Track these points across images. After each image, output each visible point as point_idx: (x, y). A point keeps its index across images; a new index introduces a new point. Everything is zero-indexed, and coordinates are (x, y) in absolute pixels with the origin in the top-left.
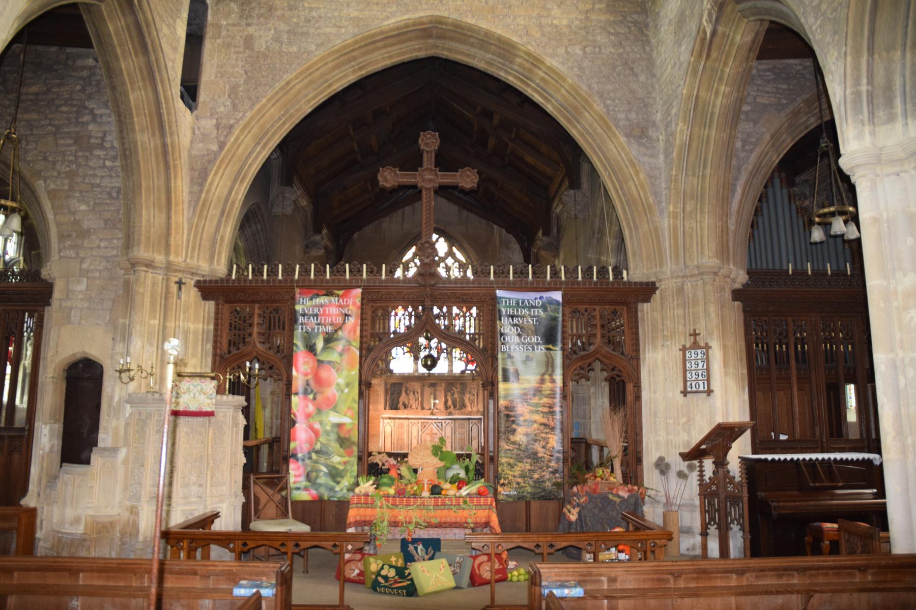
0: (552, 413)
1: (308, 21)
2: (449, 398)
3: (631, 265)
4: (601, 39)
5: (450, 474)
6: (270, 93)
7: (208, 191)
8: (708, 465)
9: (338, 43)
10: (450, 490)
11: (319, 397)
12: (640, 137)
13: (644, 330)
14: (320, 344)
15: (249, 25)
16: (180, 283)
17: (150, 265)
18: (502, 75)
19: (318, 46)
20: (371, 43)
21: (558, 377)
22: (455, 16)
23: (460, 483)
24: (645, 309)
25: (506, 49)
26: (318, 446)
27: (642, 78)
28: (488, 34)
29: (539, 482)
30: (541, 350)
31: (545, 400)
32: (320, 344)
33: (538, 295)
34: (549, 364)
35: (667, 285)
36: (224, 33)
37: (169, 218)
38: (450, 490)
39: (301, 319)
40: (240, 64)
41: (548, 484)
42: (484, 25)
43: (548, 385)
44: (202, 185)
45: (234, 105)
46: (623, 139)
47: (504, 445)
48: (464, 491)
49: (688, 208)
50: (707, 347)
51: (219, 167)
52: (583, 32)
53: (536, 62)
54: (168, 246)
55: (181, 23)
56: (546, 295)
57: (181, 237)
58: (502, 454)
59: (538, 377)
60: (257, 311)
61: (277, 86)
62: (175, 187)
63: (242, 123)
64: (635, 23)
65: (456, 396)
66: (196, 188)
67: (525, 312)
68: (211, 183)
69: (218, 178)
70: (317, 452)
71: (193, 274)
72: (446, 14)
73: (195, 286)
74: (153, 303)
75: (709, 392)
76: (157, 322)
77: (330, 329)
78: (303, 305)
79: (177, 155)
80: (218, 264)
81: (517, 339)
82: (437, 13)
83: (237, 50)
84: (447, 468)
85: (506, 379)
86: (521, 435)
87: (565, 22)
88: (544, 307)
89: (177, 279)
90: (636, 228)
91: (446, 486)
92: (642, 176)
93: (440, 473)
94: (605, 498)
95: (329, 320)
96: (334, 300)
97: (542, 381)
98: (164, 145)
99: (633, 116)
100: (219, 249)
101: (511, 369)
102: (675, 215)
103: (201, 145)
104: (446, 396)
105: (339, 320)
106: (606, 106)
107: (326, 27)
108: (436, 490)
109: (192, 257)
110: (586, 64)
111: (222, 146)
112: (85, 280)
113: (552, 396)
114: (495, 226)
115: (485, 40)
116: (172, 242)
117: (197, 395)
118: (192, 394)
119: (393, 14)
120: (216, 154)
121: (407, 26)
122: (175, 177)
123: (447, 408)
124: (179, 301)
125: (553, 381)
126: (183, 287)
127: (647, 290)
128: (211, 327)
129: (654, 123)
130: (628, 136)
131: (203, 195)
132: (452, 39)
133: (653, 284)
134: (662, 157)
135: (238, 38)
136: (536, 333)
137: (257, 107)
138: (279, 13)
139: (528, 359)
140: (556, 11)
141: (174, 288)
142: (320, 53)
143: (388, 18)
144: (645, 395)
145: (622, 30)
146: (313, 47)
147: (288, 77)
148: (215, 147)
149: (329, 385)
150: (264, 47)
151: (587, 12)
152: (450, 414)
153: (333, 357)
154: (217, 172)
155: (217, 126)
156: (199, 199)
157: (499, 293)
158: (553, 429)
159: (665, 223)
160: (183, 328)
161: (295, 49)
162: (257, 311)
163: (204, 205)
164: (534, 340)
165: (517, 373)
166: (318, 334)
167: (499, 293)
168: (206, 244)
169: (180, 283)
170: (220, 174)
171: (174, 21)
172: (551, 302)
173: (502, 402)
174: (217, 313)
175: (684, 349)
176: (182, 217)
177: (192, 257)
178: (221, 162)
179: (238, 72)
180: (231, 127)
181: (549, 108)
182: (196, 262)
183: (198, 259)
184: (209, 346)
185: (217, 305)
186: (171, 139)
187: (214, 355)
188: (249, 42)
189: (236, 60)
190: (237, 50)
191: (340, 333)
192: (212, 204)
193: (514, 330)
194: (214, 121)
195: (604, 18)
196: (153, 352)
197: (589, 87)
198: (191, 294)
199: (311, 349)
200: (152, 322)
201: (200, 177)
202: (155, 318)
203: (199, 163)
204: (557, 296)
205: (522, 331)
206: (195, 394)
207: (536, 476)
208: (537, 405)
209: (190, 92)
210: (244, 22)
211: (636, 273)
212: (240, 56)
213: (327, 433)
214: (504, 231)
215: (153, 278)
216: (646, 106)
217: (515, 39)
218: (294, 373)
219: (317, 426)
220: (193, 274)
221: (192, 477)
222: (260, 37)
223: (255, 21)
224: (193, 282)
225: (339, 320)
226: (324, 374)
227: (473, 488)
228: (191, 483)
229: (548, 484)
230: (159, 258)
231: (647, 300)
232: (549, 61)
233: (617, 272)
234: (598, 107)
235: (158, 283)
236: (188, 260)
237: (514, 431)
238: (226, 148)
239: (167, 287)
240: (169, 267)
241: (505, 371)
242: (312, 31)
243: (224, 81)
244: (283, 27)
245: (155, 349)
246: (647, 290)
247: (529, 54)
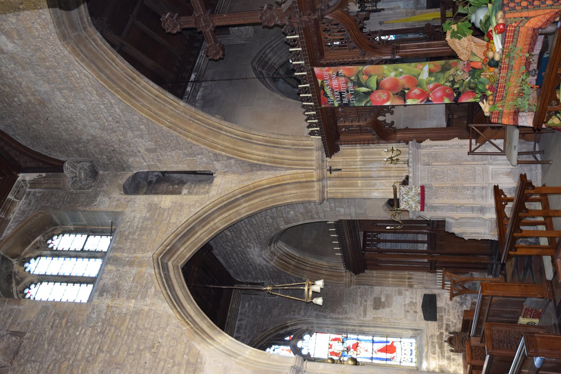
7: (264, 161)
15: (139, 152)
16: (330, 170)
40: (169, 153)
51: (245, 158)
55: (163, 203)
62: (267, 184)
68: (258, 160)
69: (253, 156)
71: (323, 161)
73: (331, 158)
76: (359, 182)
79: (246, 188)
80: (313, 146)
83: (160, 156)
89: (329, 173)
100: (302, 146)
103: (234, 168)
107: (116, 111)
109: (311, 165)
112: (337, 209)
117: (409, 197)
118: (409, 200)
120: (236, 160)
122: (262, 185)
124: (343, 170)
126: (333, 168)
131: (267, 164)
135: (151, 156)
137: (194, 142)
141: (335, 174)
148: (233, 161)
150: (150, 143)
154: (249, 158)
156: (271, 166)
160: (361, 165)
163: (274, 163)
170: (250, 155)
171: (164, 210)
176: (285, 175)
177: (311, 165)
178: (241, 157)
179: (175, 154)
180: (215, 155)
182: (314, 162)
183: (312, 160)
185: (341, 144)
186: (238, 195)
189: (168, 156)
190: (160, 156)
192: (271, 155)
194: (214, 162)
196: (380, 183)
198: (337, 160)
200: (360, 185)
202: (357, 183)
203: (246, 168)
206: (409, 198)
212: (163, 154)
215: (330, 187)
220: (323, 161)
221: (468, 193)
222: (145, 145)
223: (135, 149)
224: (328, 159)
228: (472, 194)
235: (334, 183)
236: (314, 168)
238: (231, 156)
239: (335, 178)
243: (185, 160)
244: (130, 134)
245: (378, 181)
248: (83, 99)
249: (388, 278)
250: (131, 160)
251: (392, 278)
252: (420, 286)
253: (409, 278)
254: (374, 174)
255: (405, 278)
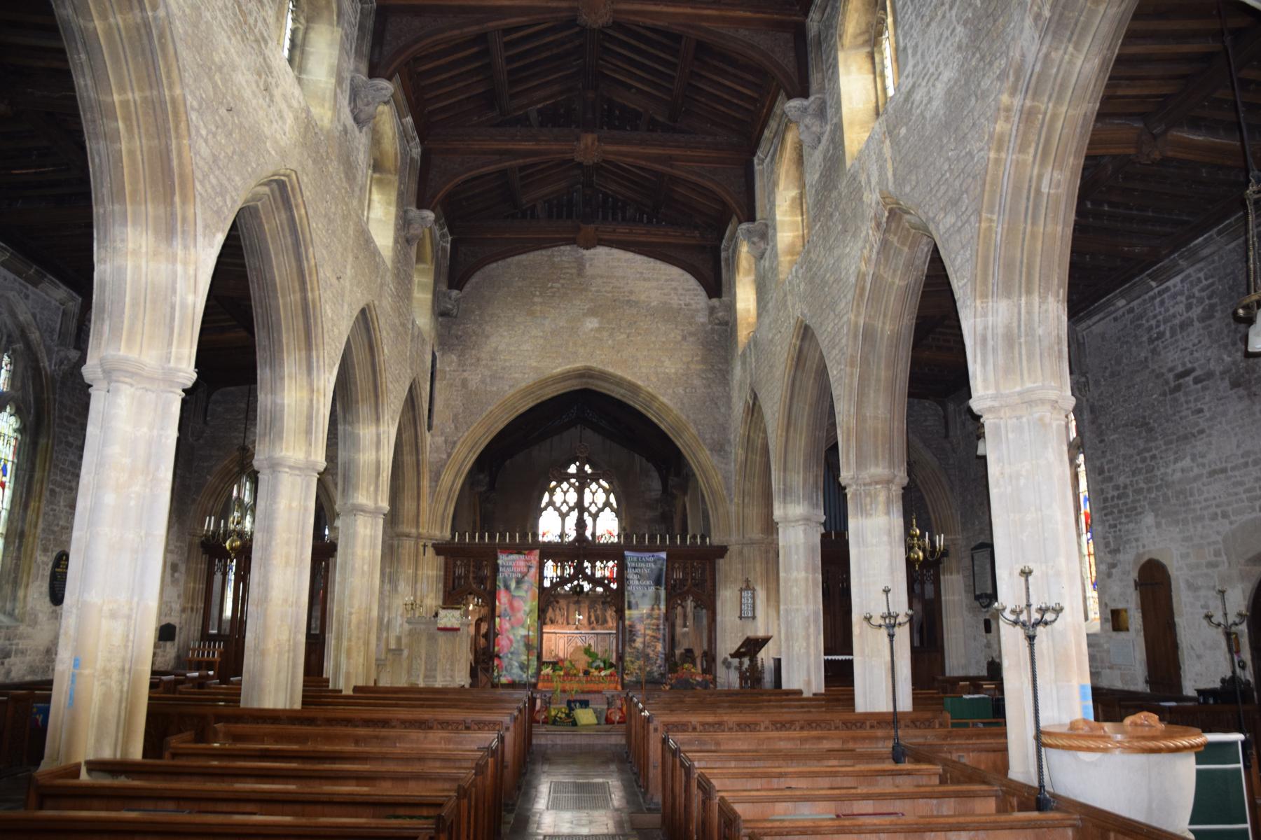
0: (658, 629)
1: (504, 368)
2: (592, 614)
3: (713, 534)
4: (697, 382)
5: (595, 665)
6: (480, 419)
8: (746, 661)
9: (523, 385)
10: (595, 672)
11: (513, 619)
12: (720, 451)
13: (719, 577)
14: (513, 585)
15: (464, 371)
16: (425, 546)
17: (408, 536)
18: (631, 403)
19: (510, 387)
20: (544, 383)
21: (663, 607)
22: (600, 367)
23: (599, 669)
24: (721, 562)
25: (634, 388)
26: (512, 649)
27: (723, 410)
28: (621, 379)
29: (650, 673)
30: (652, 589)
31: (654, 621)
32: (513, 585)
33: (651, 554)
34: (657, 598)
35: (733, 549)
36: (448, 376)
37: (418, 505)
38: (595, 672)
39: (501, 569)
40: (460, 399)
41: (656, 674)
42: (619, 373)
43: (656, 612)
44: (437, 481)
45: (456, 428)
46: (708, 452)
47: (628, 649)
48: (603, 673)
49: (746, 501)
50: (754, 590)
52: (685, 378)
53: (653, 398)
54: (418, 522)
56: (656, 554)
57: (425, 517)
58: (627, 655)
59: (650, 607)
60: (472, 564)
61: (484, 415)
63: (462, 440)
64: (720, 370)
65: (599, 612)
66: (434, 484)
67: (643, 565)
70: (512, 653)
72: (594, 365)
74: (409, 559)
75: (754, 617)
77: (519, 575)
78: (503, 560)
81: (637, 582)
82: (588, 364)
84: (593, 662)
85: (630, 608)
86: (639, 643)
87: (673, 371)
88: (655, 562)
90: (716, 509)
91: (593, 670)
92: (720, 477)
93: (590, 665)
94: (687, 682)
95: (519, 570)
96: (522, 557)
97: (653, 609)
98: (418, 461)
99: (716, 436)
101: (633, 601)
102: (738, 505)
104: (589, 613)
105: (526, 570)
106: (698, 430)
108: (586, 673)
110: (685, 400)
111: (449, 456)
113: (658, 619)
114: (636, 455)
115: (620, 382)
116: (421, 520)
119: (560, 365)
121: (569, 372)
123: (590, 623)
125: (659, 609)
127: (722, 551)
128: (442, 573)
129: (729, 441)
130: (711, 450)
132: (598, 379)
133: (726, 547)
134: (733, 464)
136: (649, 578)
137: (471, 429)
138: (484, 362)
139: (644, 595)
140: (667, 363)
141: (421, 549)
142: (512, 391)
143: (556, 367)
144: (719, 618)
145: (710, 375)
146: (507, 388)
147: (490, 408)
148: (444, 456)
149: (519, 610)
151: (688, 363)
152: (593, 629)
153: (522, 593)
155: (446, 442)
157: (626, 553)
158: (658, 639)
159: (733, 509)
161: (495, 389)
162: (472, 564)
164: (648, 583)
165: (637, 604)
166: (511, 579)
167: (626, 553)
168: (439, 519)
169: (425, 546)
172: (659, 559)
173: (627, 622)
174: (446, 564)
175: (741, 590)
176: (425, 504)
180: (455, 443)
181: (662, 427)
184: (441, 586)
185: (446, 559)
187: (445, 592)
188: (464, 383)
191: (526, 578)
193: (635, 577)
195: (699, 367)
197: (688, 417)
198: (430, 552)
199: (507, 588)
201: (436, 477)
204: (664, 555)
205: (641, 577)
207: (648, 669)
208: (649, 624)
209: (430, 428)
210: (461, 369)
211: (716, 539)
213: (518, 641)
214: (644, 460)
216: (724, 429)
217: (640, 383)
218: (497, 603)
219: (511, 637)
225: (526, 570)
226: (516, 604)
227: (608, 672)
229: (656, 674)
230: (414, 531)
231: (722, 556)
232: (662, 399)
233: (703, 538)
234: (693, 430)
237: (634, 641)
240: (419, 537)
241: (629, 603)
242: (506, 376)
244: (487, 373)
246: (722, 551)
247: (649, 393)
248: (533, 351)
249: (195, 583)
250: (454, 357)
251: (194, 588)
252: (183, 622)
253: (192, 609)
254: (419, 586)
255: (193, 602)
